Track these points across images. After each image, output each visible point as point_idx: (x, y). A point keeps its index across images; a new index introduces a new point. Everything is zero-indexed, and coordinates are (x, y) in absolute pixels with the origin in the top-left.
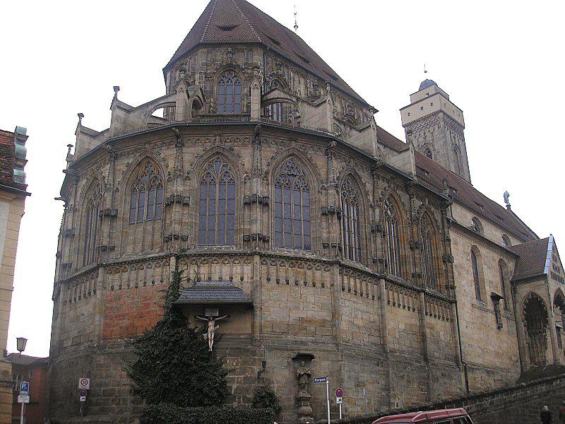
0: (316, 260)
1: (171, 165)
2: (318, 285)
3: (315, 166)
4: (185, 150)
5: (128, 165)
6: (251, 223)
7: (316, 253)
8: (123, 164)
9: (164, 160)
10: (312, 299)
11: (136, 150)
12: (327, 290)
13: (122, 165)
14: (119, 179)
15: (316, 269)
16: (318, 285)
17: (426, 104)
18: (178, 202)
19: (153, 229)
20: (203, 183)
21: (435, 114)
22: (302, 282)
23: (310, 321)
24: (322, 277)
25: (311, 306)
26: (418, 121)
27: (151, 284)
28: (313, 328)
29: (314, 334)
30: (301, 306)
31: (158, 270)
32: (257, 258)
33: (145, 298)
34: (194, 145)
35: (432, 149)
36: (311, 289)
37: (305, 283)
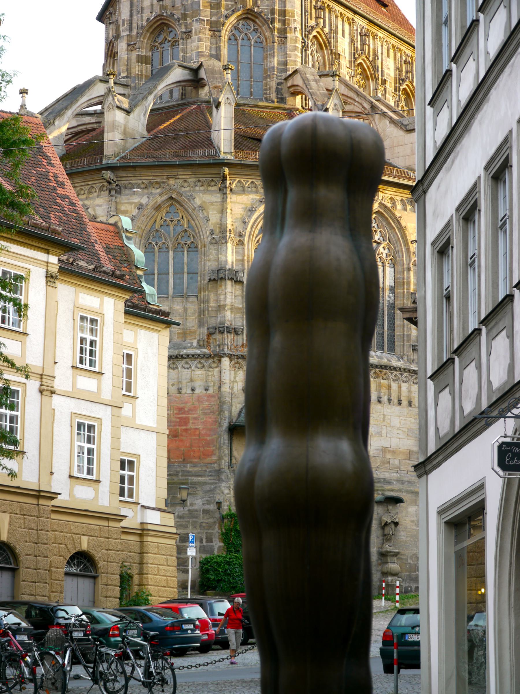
0: (405, 369)
1: (214, 218)
2: (405, 403)
7: (402, 358)
8: (131, 203)
9: (202, 208)
10: (396, 422)
12: (414, 411)
15: (403, 382)
16: (405, 403)
18: (232, 279)
19: (185, 310)
22: (385, 399)
23: (394, 452)
24: (410, 391)
25: (396, 431)
27: (189, 391)
28: (397, 462)
29: (398, 469)
30: (384, 432)
31: (200, 373)
33: (180, 409)
36: (397, 409)
37: (389, 400)
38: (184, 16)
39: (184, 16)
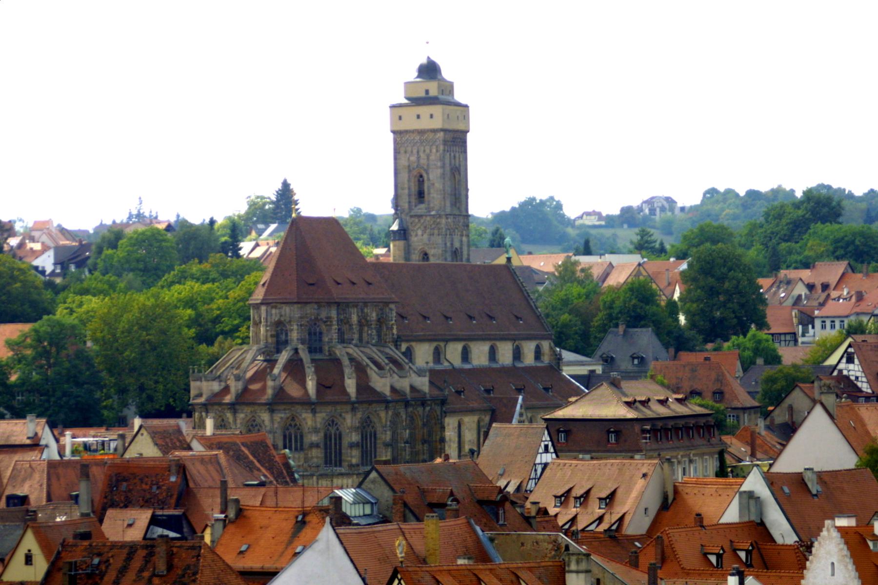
1: (310, 423)
3: (380, 418)
4: (317, 415)
5: (281, 418)
6: (352, 457)
9: (304, 419)
11: (285, 410)
13: (278, 417)
14: (276, 426)
17: (425, 110)
20: (325, 435)
21: (434, 131)
26: (413, 131)
32: (355, 477)
34: (321, 412)
35: (425, 175)
38: (290, 321)
39: (290, 321)
